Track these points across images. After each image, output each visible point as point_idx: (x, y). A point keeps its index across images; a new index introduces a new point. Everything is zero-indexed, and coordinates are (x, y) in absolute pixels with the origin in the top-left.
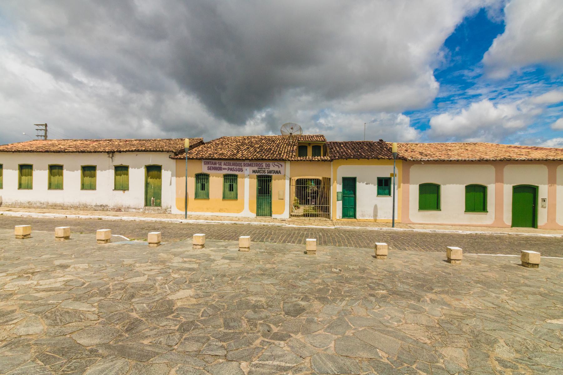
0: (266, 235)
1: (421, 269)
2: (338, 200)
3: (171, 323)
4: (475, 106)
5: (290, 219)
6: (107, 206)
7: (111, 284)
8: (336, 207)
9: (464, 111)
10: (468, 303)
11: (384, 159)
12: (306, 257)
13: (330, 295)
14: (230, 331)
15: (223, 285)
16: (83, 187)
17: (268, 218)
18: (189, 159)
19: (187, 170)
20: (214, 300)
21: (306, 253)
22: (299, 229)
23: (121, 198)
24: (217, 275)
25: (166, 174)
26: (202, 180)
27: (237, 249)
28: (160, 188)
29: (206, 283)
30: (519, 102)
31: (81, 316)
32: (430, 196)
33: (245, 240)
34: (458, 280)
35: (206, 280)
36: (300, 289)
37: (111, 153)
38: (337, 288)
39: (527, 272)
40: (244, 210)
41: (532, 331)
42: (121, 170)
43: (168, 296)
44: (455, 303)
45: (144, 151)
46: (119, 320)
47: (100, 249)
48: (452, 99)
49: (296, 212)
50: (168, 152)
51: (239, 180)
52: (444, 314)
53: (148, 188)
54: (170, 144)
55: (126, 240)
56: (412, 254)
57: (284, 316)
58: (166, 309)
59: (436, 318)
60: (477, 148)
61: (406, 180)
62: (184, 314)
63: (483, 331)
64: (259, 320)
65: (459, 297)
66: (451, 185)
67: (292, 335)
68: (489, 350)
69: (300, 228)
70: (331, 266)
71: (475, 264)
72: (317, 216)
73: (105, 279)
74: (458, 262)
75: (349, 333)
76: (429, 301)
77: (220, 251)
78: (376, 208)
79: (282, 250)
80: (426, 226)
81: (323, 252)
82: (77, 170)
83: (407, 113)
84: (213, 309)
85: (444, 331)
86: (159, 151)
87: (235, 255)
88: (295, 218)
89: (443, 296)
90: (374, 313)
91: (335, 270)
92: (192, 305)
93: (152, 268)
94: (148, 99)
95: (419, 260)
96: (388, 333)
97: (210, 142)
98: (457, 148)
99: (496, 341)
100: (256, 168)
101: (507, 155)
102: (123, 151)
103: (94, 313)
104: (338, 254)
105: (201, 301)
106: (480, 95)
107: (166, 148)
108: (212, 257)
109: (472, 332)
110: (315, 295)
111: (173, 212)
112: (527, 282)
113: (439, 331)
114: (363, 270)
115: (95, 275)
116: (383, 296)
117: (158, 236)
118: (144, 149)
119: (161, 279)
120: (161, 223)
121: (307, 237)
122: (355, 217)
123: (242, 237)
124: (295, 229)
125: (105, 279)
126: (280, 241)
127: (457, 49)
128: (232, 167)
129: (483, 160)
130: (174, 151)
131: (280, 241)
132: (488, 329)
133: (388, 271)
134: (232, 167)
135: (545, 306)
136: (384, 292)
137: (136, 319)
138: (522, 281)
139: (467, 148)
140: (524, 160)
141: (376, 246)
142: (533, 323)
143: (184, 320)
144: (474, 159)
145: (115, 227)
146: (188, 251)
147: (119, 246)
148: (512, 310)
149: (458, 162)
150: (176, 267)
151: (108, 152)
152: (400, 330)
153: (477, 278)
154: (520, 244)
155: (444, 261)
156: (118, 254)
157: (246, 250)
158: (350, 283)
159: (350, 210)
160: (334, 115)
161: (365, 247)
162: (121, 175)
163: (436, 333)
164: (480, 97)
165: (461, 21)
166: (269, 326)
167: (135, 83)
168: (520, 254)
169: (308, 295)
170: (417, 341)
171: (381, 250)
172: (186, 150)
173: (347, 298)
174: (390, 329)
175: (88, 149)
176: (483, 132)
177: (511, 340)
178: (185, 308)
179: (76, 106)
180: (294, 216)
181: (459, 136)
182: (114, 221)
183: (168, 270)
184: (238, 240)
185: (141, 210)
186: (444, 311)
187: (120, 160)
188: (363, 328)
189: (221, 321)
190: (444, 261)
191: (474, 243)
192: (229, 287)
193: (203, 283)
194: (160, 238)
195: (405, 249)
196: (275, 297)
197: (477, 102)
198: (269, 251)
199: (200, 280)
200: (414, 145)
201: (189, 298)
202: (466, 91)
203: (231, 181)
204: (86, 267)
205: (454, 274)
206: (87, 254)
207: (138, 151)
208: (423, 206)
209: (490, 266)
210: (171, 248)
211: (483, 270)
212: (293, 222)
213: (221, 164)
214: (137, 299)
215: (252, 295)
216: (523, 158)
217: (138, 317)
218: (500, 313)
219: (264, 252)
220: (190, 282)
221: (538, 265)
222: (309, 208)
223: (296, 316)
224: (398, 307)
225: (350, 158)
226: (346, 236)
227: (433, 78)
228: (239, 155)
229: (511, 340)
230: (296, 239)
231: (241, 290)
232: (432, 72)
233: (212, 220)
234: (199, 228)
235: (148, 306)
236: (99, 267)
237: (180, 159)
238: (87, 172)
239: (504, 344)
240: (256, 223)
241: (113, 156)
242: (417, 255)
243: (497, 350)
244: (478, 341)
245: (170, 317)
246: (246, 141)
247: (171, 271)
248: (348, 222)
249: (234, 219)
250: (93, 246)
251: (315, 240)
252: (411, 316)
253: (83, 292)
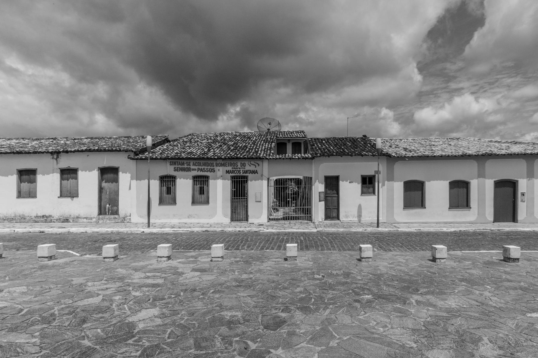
0: (242, 242)
1: (406, 270)
2: (320, 201)
3: (132, 349)
4: (457, 100)
5: (268, 224)
6: (50, 216)
7: (56, 308)
8: (318, 209)
9: (446, 105)
10: (452, 302)
11: (368, 155)
12: (286, 265)
13: (313, 304)
14: (202, 352)
15: (194, 301)
16: (20, 195)
17: (244, 224)
18: (152, 159)
19: (149, 172)
20: (183, 318)
21: (286, 259)
22: (278, 234)
23: (68, 207)
24: (186, 290)
25: (124, 178)
26: (168, 183)
27: (210, 259)
28: (117, 193)
29: (173, 300)
30: (499, 96)
31: (18, 349)
32: (415, 194)
33: (218, 249)
34: (443, 279)
35: (173, 296)
36: (281, 300)
37: (56, 154)
38: (320, 296)
39: (508, 267)
40: (216, 214)
41: (513, 327)
42: (68, 173)
43: (128, 318)
44: (440, 303)
45: (98, 151)
46: (66, 350)
47: (42, 268)
48: (435, 92)
49: (275, 215)
50: (126, 151)
51: (211, 182)
52: (430, 316)
53: (103, 194)
54: (129, 142)
55: (75, 255)
56: (398, 255)
57: (263, 330)
58: (126, 333)
59: (422, 320)
60: (460, 143)
61: (391, 178)
62: (147, 337)
63: (467, 330)
64: (235, 337)
65: (444, 296)
66: (435, 182)
67: (272, 350)
68: (474, 349)
69: (279, 232)
70: (313, 272)
71: (459, 261)
72: (298, 219)
73: (48, 304)
74: (443, 261)
75: (333, 343)
76: (415, 304)
77: (189, 263)
78: (360, 207)
79: (260, 258)
80: (411, 225)
81: (305, 258)
82: (12, 175)
83: (391, 106)
84: (182, 329)
85: (430, 333)
86: (116, 151)
87: (207, 266)
88: (274, 222)
89: (428, 297)
90: (359, 320)
91: (318, 276)
92: (156, 326)
93: (108, 286)
94: (101, 90)
95: (404, 261)
96: (374, 340)
97: (177, 140)
98: (441, 143)
99: (480, 339)
100: (230, 168)
101: (488, 150)
102: (71, 152)
103: (34, 344)
104: (320, 258)
105: (168, 321)
106: (462, 89)
107: (124, 147)
108: (180, 270)
109: (457, 332)
110: (297, 305)
111: (132, 221)
112: (508, 277)
113: (425, 333)
114: (347, 275)
115: (36, 299)
116: (369, 301)
117: (115, 249)
118: (97, 148)
119: (119, 299)
120: (118, 233)
121: (288, 242)
122: (338, 218)
123: (214, 246)
124: (273, 234)
125: (48, 304)
126: (257, 248)
127: (440, 41)
128: (203, 167)
129: (465, 155)
130: (134, 150)
131: (257, 248)
132: (472, 327)
133: (373, 275)
134: (203, 167)
135: (526, 300)
136: (370, 297)
137: (89, 348)
138: (504, 277)
139: (450, 143)
140: (505, 155)
141: (361, 248)
142: (514, 318)
143: (147, 344)
144: (457, 154)
145: (62, 241)
146: (151, 265)
147: (66, 263)
148: (495, 307)
149: (441, 157)
150: (137, 283)
151: (52, 153)
152: (386, 336)
153: (461, 276)
154: (501, 240)
155: (430, 260)
156: (66, 272)
157: (220, 259)
158: (334, 290)
159: (332, 212)
160: (315, 109)
161: (349, 250)
162: (68, 180)
163: (422, 336)
164: (463, 91)
165: (444, 13)
166: (246, 343)
167: (85, 73)
168: (502, 249)
169: (289, 305)
170: (403, 346)
171: (366, 252)
172: (148, 149)
173: (331, 306)
174: (376, 336)
175: (26, 150)
176: (465, 126)
177: (494, 337)
178: (148, 330)
179: (10, 97)
180: (272, 219)
181: (445, 130)
182: (59, 234)
183: (127, 288)
184: (210, 249)
185: (94, 220)
186: (430, 313)
187: (66, 162)
188: (348, 337)
189: (192, 341)
190: (430, 260)
191: (459, 240)
192: (200, 303)
193: (169, 300)
194: (117, 251)
195: (390, 250)
196: (253, 310)
197: (459, 96)
198: (245, 260)
199: (166, 297)
200: (398, 141)
201: (153, 318)
202: (449, 84)
203: (201, 185)
204: (24, 291)
205: (439, 274)
206: (25, 275)
207: (90, 151)
208: (408, 204)
209: (473, 263)
210: (131, 263)
211: (467, 267)
212: (272, 226)
213: (189, 165)
214: (89, 324)
215: (227, 310)
216: (503, 152)
217: (90, 345)
218: (483, 310)
219: (240, 261)
220: (154, 300)
221: (518, 259)
222: (289, 210)
223: (276, 329)
224: (384, 312)
225: (332, 155)
226: (329, 240)
227: (416, 70)
228: (211, 154)
229: (494, 337)
230: (275, 245)
231: (214, 305)
232: (415, 65)
233: (180, 228)
234: (164, 238)
235: (103, 331)
236: (41, 289)
237: (141, 159)
238: (24, 177)
239: (488, 342)
240: (230, 229)
241: (58, 157)
242: (402, 255)
243: (482, 349)
244: (463, 341)
245: (130, 342)
246: (219, 138)
247: (131, 288)
248: (331, 225)
249: (205, 226)
250: (33, 264)
251: (296, 245)
252: (397, 319)
253: (21, 320)
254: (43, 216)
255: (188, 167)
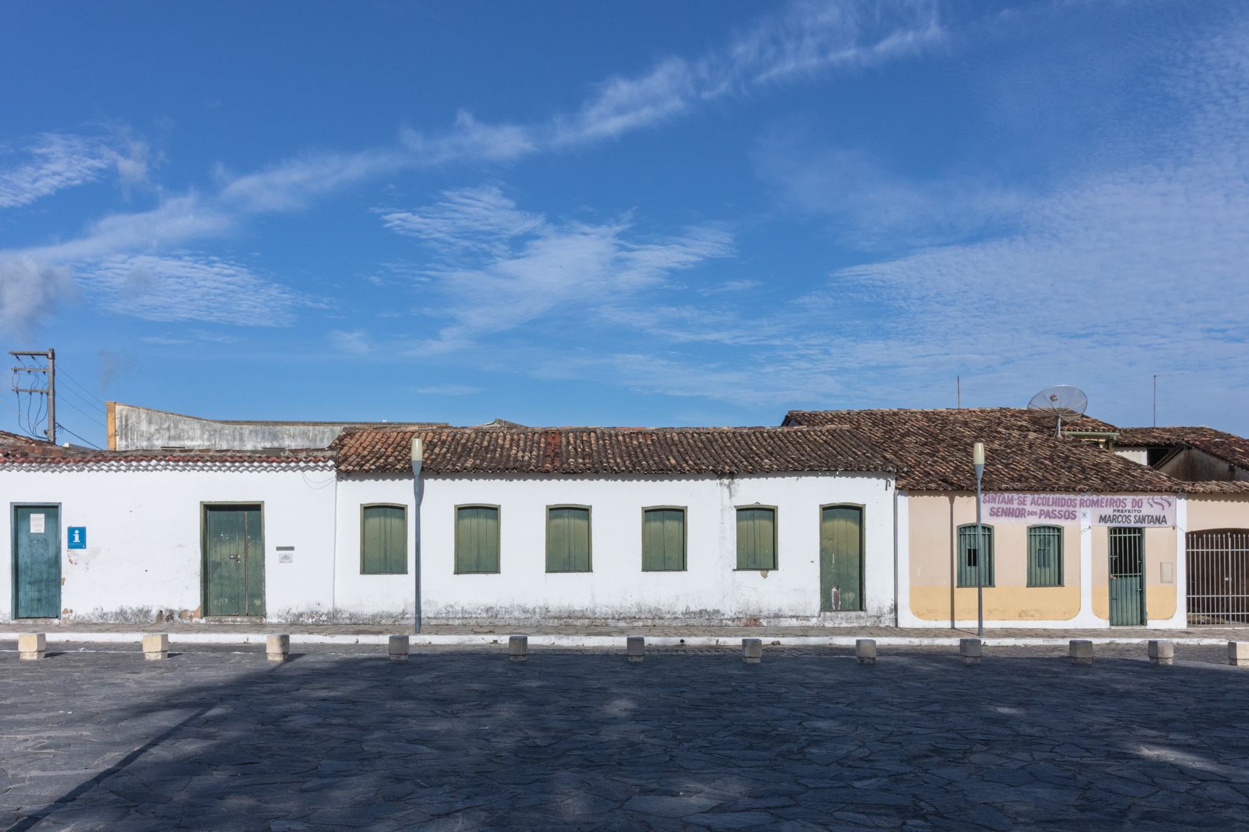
100: (1108, 511)
128: (1050, 509)
134: (1050, 509)
254: (701, 612)
255: (1021, 507)
